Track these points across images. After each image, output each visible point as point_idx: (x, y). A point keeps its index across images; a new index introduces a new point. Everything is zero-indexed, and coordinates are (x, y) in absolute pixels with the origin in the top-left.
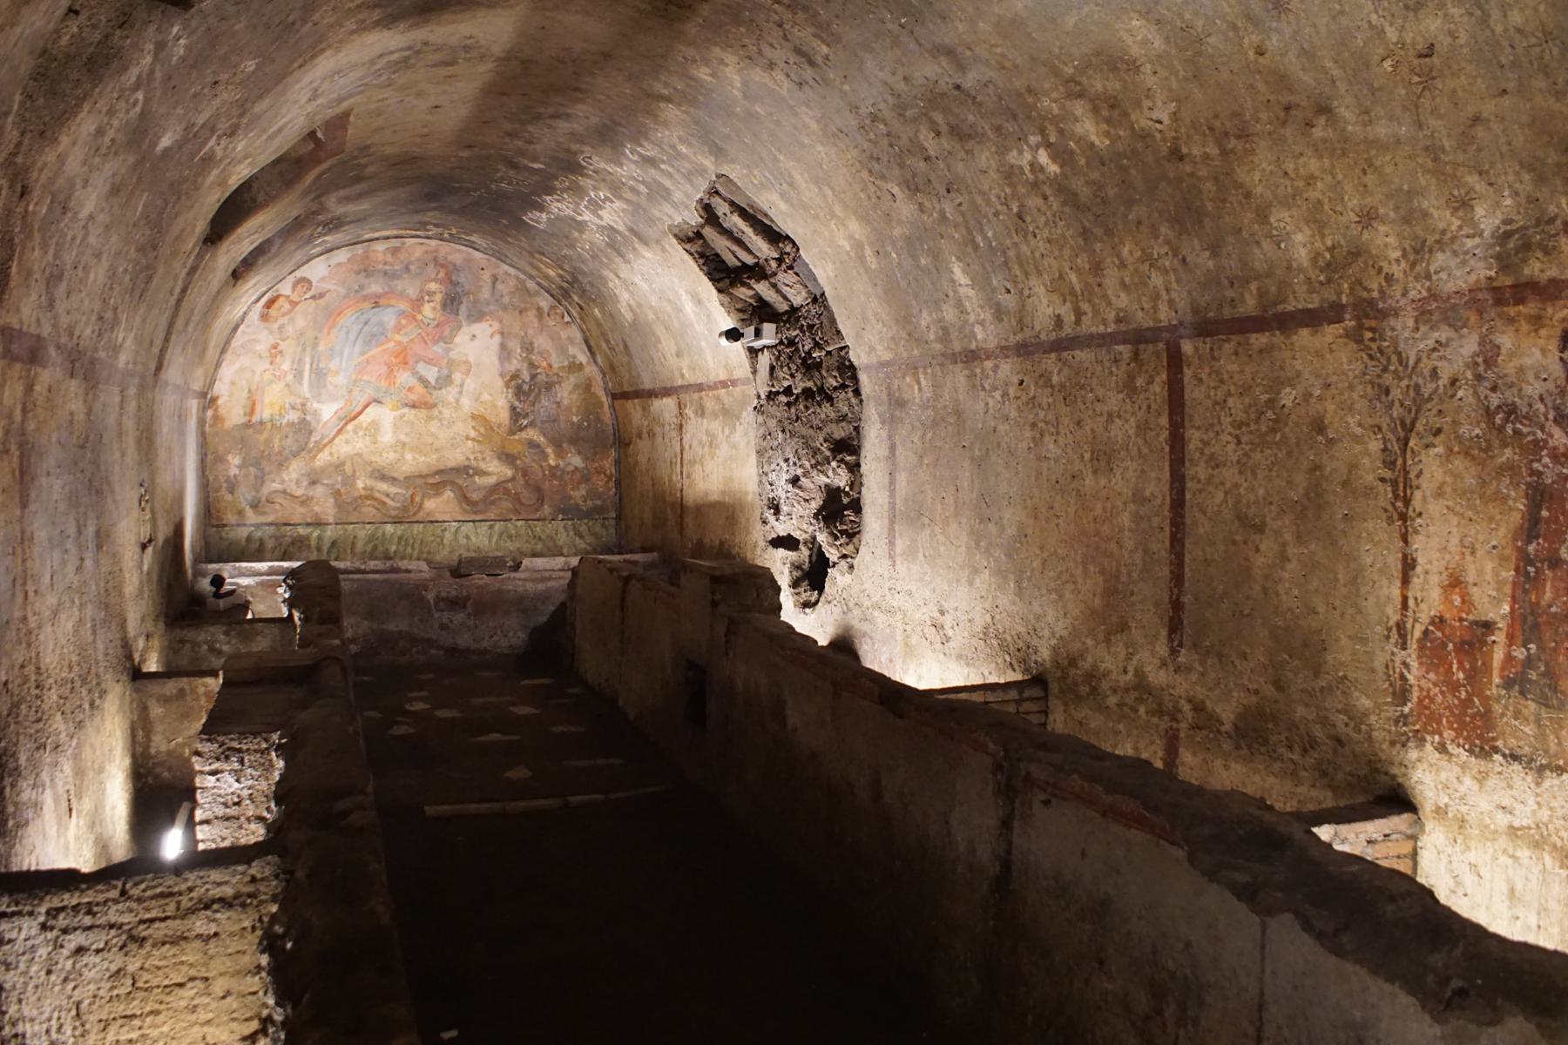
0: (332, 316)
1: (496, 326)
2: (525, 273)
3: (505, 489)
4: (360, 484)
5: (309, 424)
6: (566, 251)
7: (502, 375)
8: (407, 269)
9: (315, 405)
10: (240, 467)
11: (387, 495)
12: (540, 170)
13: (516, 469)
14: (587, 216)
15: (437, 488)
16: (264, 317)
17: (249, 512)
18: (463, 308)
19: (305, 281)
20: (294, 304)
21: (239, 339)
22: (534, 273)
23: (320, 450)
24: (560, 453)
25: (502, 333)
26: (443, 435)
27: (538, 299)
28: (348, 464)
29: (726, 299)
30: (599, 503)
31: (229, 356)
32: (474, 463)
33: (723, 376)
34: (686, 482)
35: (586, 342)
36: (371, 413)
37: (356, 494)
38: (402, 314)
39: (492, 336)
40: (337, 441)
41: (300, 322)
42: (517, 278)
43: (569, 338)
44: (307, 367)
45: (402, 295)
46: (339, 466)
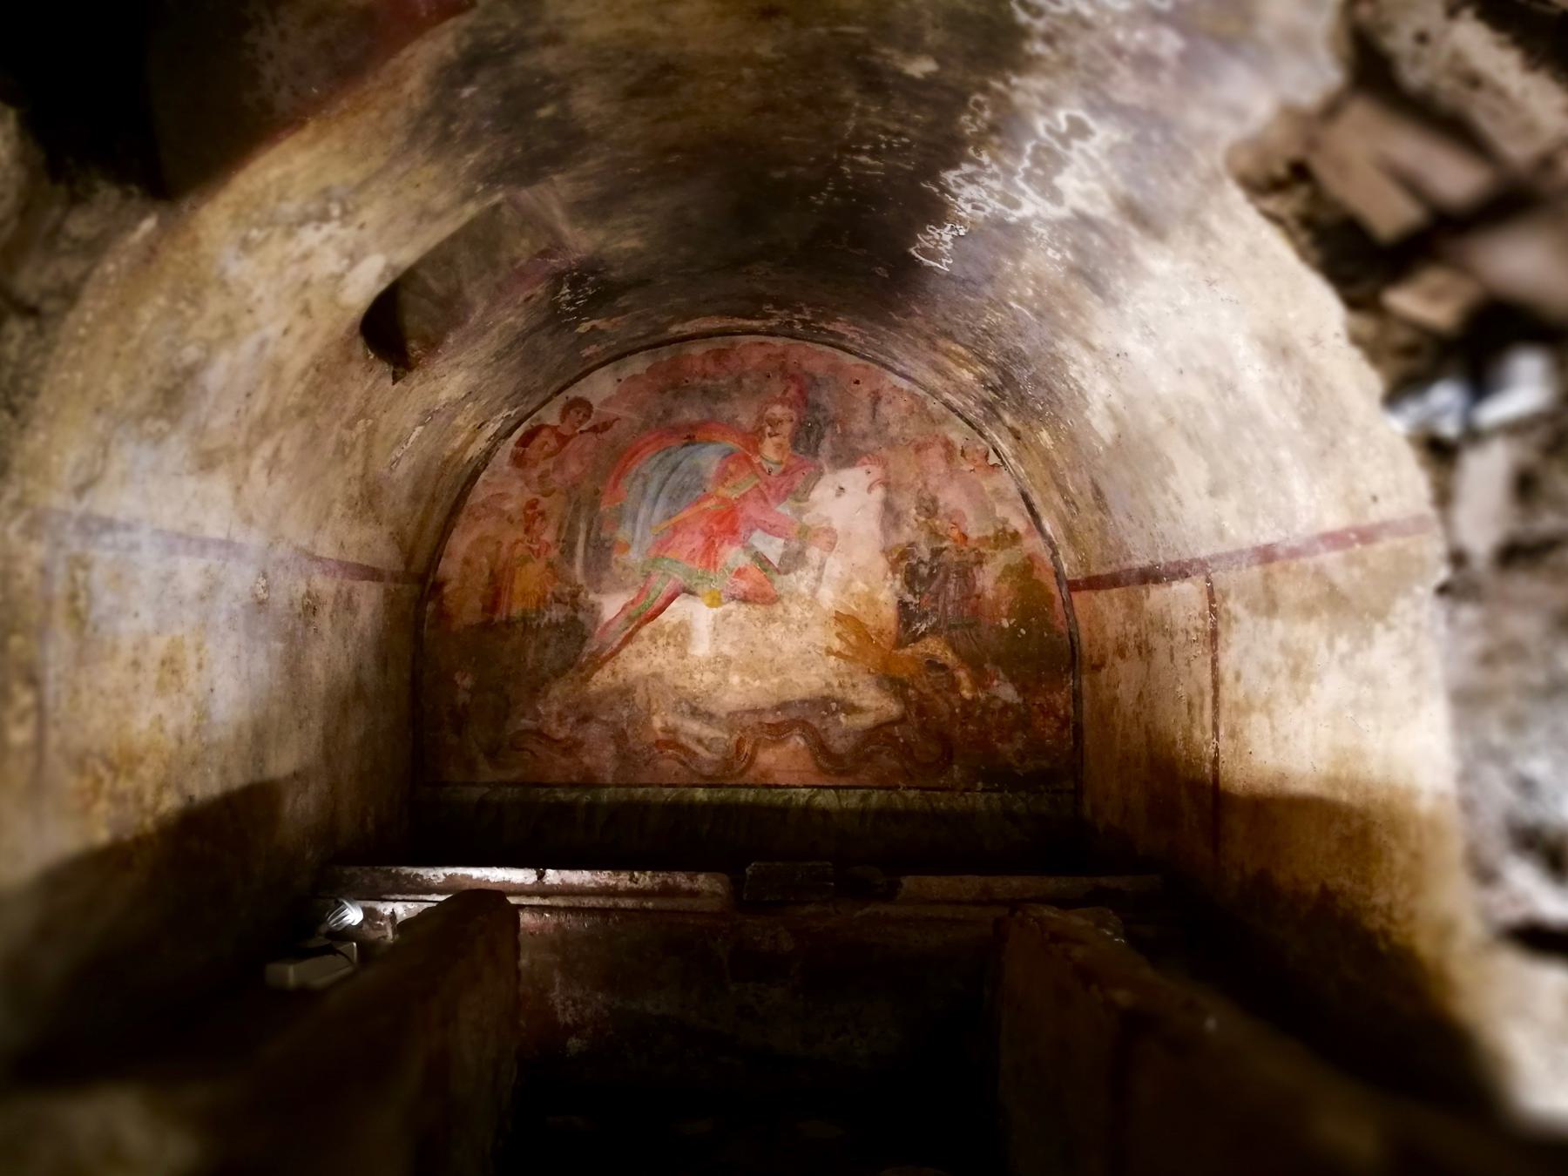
0: (619, 460)
1: (877, 472)
2: (924, 387)
3: (890, 736)
4: (657, 723)
5: (582, 625)
6: (992, 318)
7: (886, 552)
8: (739, 381)
9: (592, 597)
10: (472, 692)
11: (700, 741)
12: (929, 82)
13: (906, 701)
14: (1031, 206)
15: (778, 732)
16: (518, 460)
17: (483, 766)
18: (826, 445)
19: (582, 405)
20: (563, 440)
21: (480, 493)
22: (936, 382)
23: (599, 667)
24: (980, 681)
25: (886, 485)
26: (791, 646)
27: (946, 428)
28: (640, 690)
29: (1367, 326)
30: (1045, 764)
31: (462, 518)
32: (839, 693)
33: (1334, 520)
34: (1225, 744)
35: (1025, 497)
36: (679, 609)
37: (652, 739)
38: (730, 455)
39: (870, 489)
40: (624, 652)
41: (573, 468)
42: (913, 395)
43: (996, 491)
44: (581, 538)
45: (731, 426)
46: (625, 693)
